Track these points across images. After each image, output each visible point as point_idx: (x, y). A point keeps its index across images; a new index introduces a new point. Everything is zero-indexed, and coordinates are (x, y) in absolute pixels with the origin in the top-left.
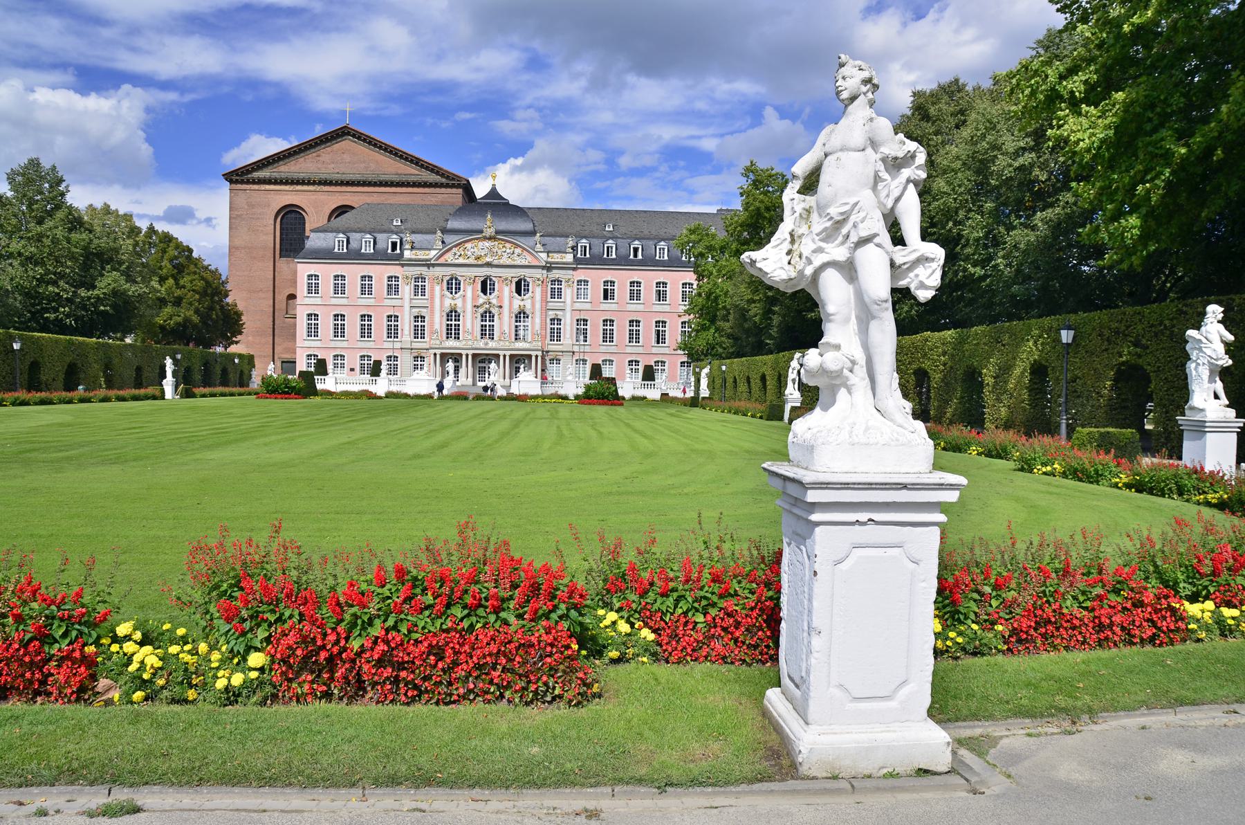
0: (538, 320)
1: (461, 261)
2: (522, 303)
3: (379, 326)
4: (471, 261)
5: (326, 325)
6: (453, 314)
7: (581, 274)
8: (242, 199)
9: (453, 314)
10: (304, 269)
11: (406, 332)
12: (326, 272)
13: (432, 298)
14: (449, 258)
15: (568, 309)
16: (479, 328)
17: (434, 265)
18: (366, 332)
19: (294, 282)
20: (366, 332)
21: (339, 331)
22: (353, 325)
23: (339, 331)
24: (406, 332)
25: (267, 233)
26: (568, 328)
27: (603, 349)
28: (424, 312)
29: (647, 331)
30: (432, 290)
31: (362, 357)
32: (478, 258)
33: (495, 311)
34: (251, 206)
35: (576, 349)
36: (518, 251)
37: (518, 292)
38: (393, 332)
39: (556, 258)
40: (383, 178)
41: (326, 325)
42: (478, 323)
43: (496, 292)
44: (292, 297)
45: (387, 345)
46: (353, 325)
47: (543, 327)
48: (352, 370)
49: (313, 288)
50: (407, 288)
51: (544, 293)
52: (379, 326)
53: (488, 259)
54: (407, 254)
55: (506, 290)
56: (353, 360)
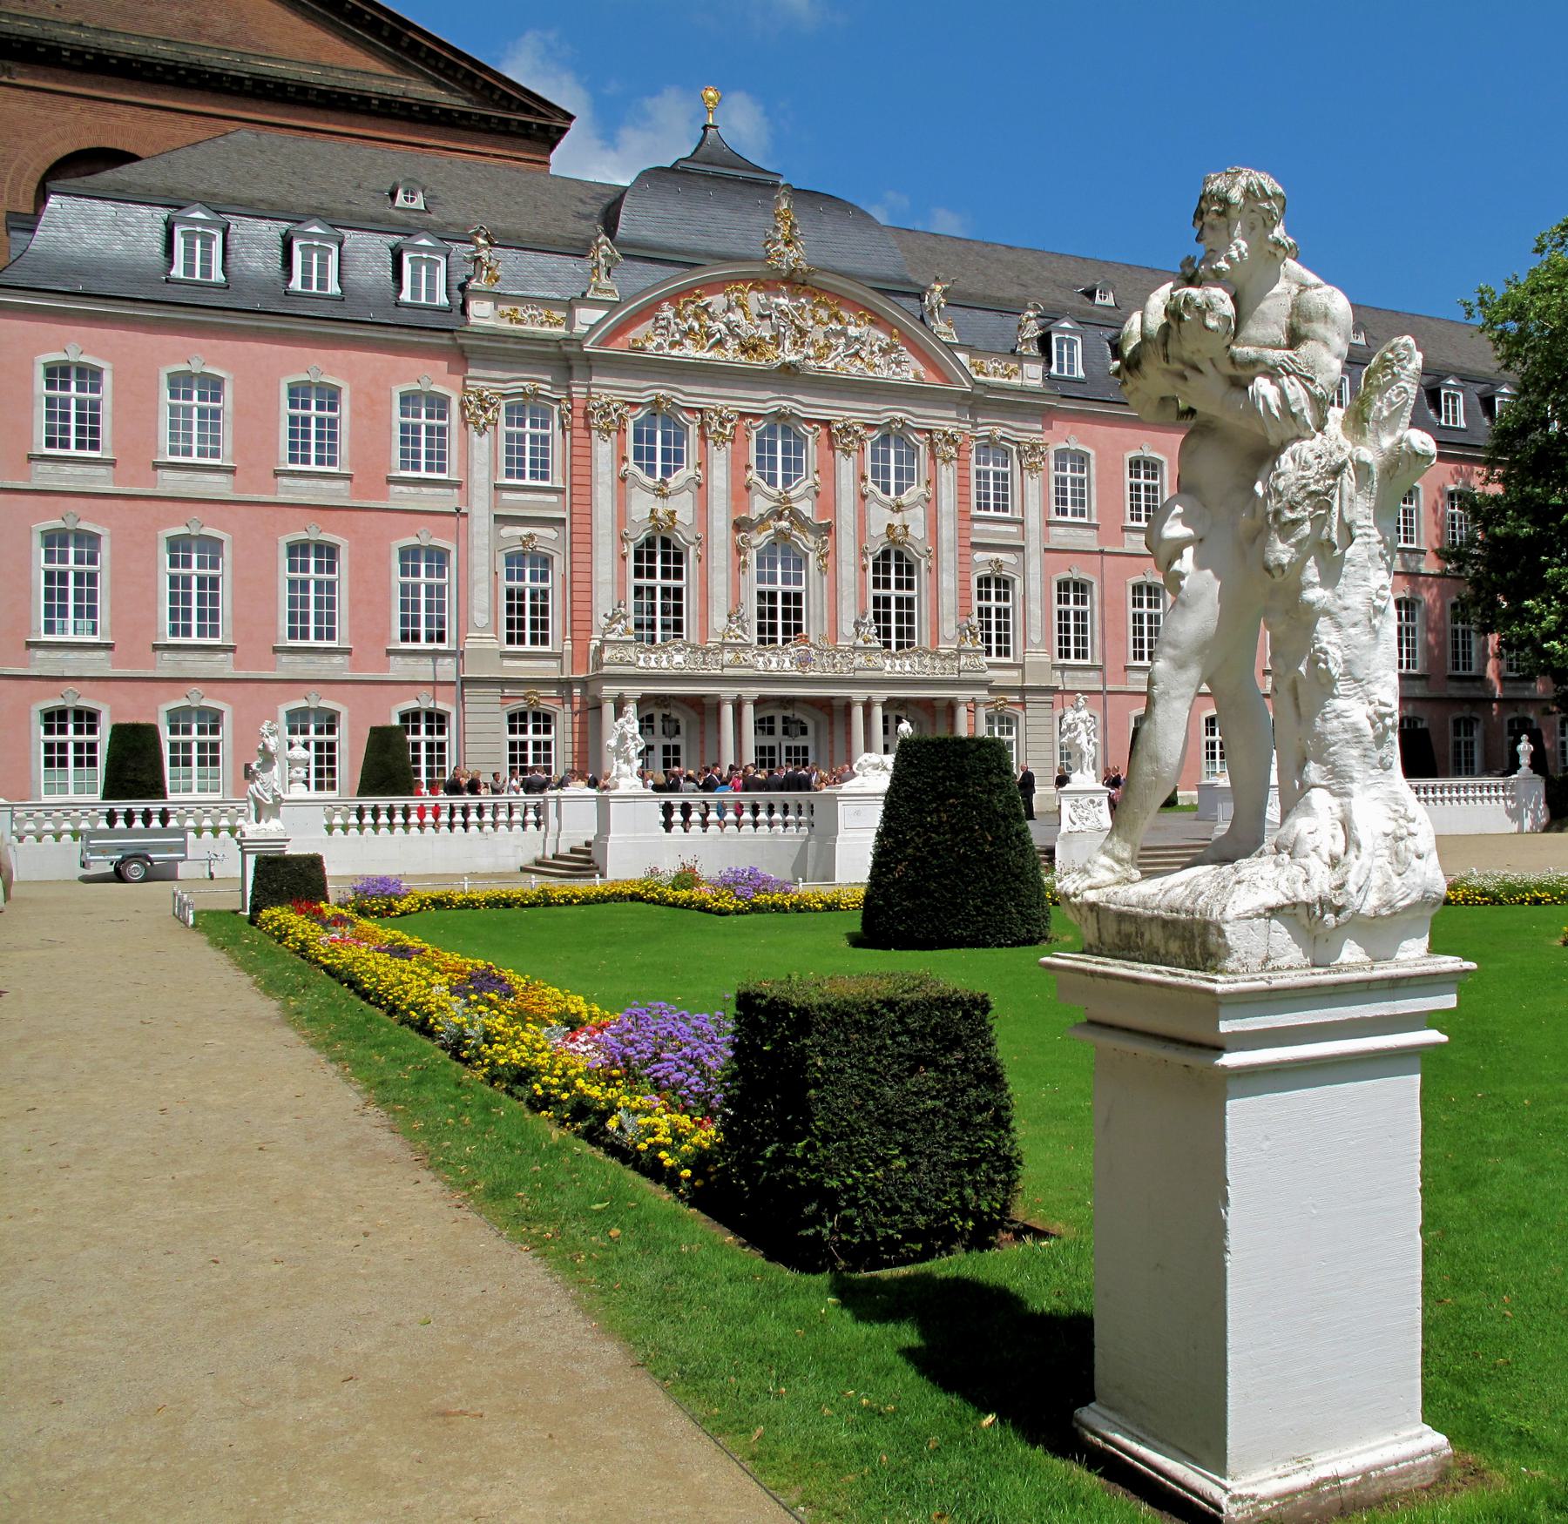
0: (948, 581)
2: (896, 520)
4: (731, 355)
7: (1065, 436)
9: (660, 552)
13: (580, 486)
14: (649, 339)
15: (1034, 546)
16: (751, 607)
17: (591, 364)
24: (480, 617)
26: (1035, 608)
33: (807, 542)
37: (880, 473)
40: (264, 67)
45: (399, 669)
50: (481, 445)
51: (963, 482)
54: (482, 313)
55: (846, 468)
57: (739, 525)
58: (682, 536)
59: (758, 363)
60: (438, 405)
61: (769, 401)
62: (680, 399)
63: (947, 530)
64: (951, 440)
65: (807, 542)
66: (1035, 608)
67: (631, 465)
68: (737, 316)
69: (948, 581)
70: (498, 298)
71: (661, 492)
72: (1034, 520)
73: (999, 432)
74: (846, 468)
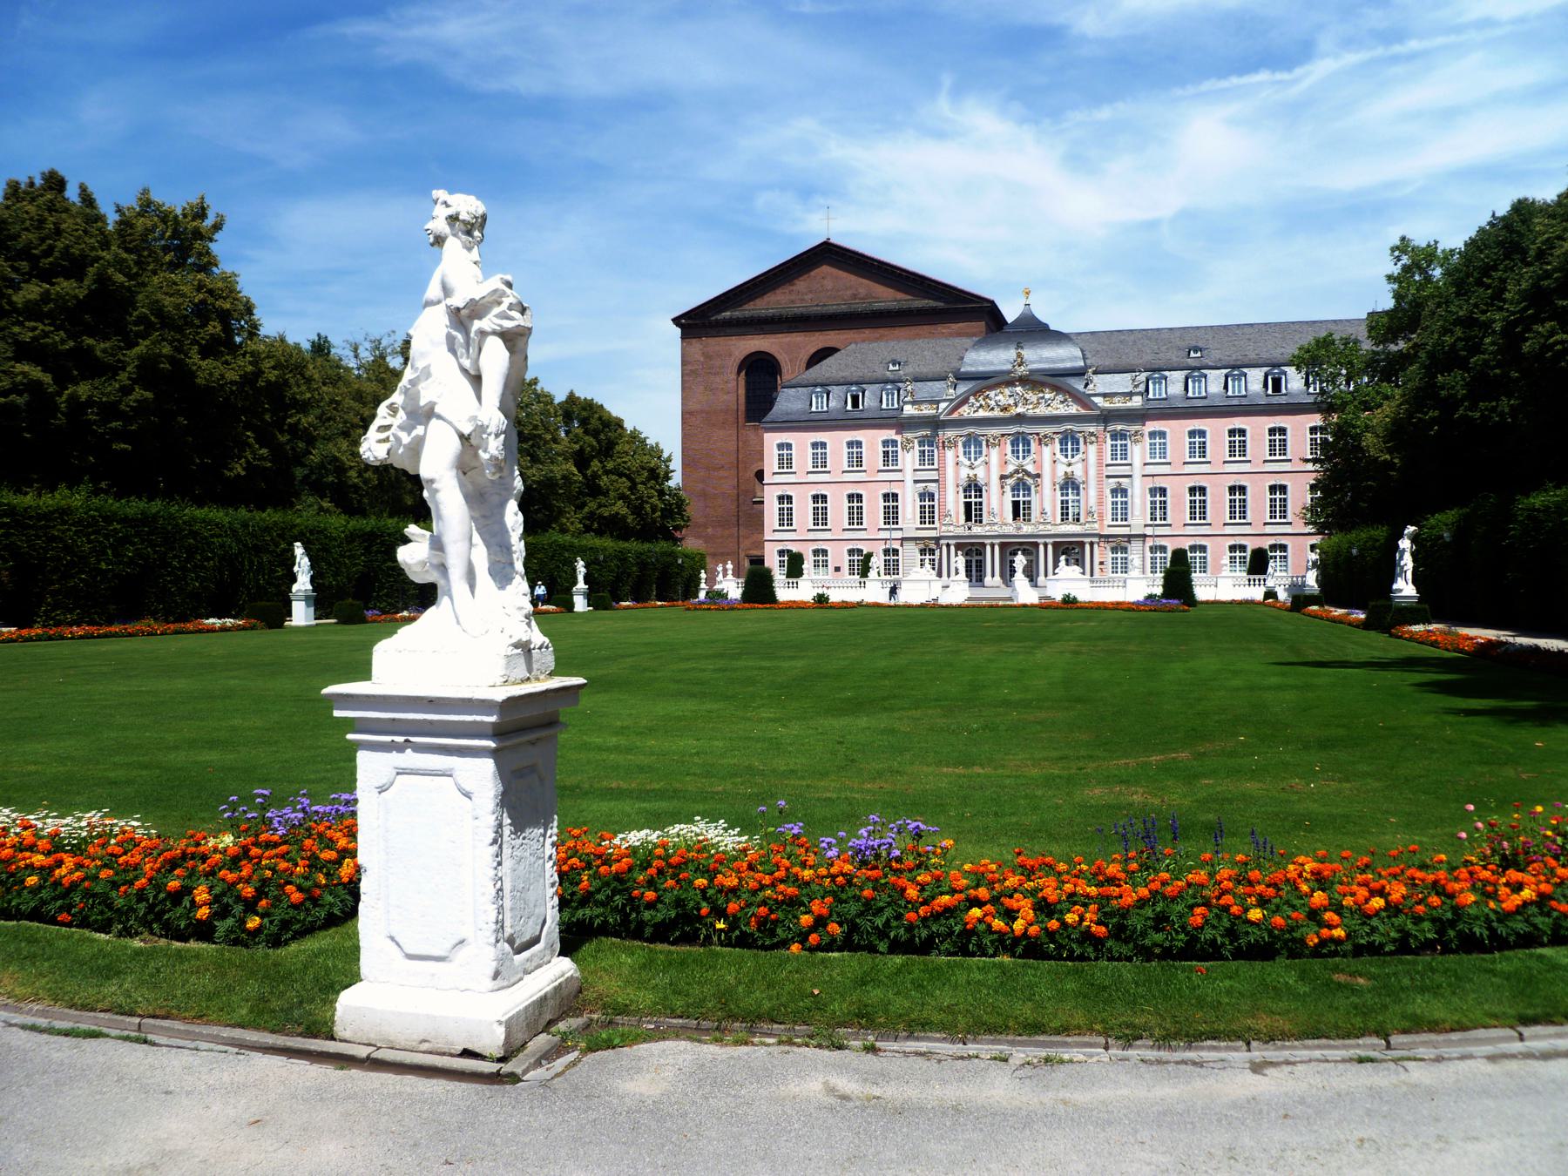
0: (1092, 492)
1: (982, 413)
2: (1069, 470)
3: (874, 509)
4: (997, 413)
5: (803, 511)
6: (973, 488)
8: (697, 346)
9: (973, 488)
10: (772, 440)
11: (909, 515)
12: (801, 441)
14: (966, 412)
15: (1137, 471)
18: (856, 516)
19: (760, 456)
20: (856, 516)
21: (820, 517)
22: (838, 509)
23: (820, 517)
24: (909, 515)
25: (731, 389)
27: (1190, 530)
28: (932, 487)
29: (1258, 501)
30: (942, 460)
31: (851, 552)
32: (1004, 409)
33: (1030, 481)
34: (708, 356)
35: (1149, 531)
36: (1060, 397)
37: (1064, 451)
38: (891, 516)
39: (1118, 404)
41: (803, 511)
42: (1009, 498)
43: (1033, 456)
44: (760, 475)
46: (838, 509)
47: (1100, 503)
48: (837, 569)
49: (785, 462)
50: (909, 456)
51: (1100, 452)
52: (874, 509)
53: (1020, 410)
56: (839, 555)
57: (1003, 477)
58: (981, 482)
59: (1007, 414)
60: (894, 443)
61: (1014, 429)
62: (978, 432)
63: (1092, 472)
64: (1092, 434)
65: (1030, 481)
66: (1137, 501)
67: (962, 458)
68: (1000, 397)
69: (1092, 492)
70: (913, 403)
71: (971, 467)
72: (1137, 463)
73: (1119, 428)
74: (1047, 451)
